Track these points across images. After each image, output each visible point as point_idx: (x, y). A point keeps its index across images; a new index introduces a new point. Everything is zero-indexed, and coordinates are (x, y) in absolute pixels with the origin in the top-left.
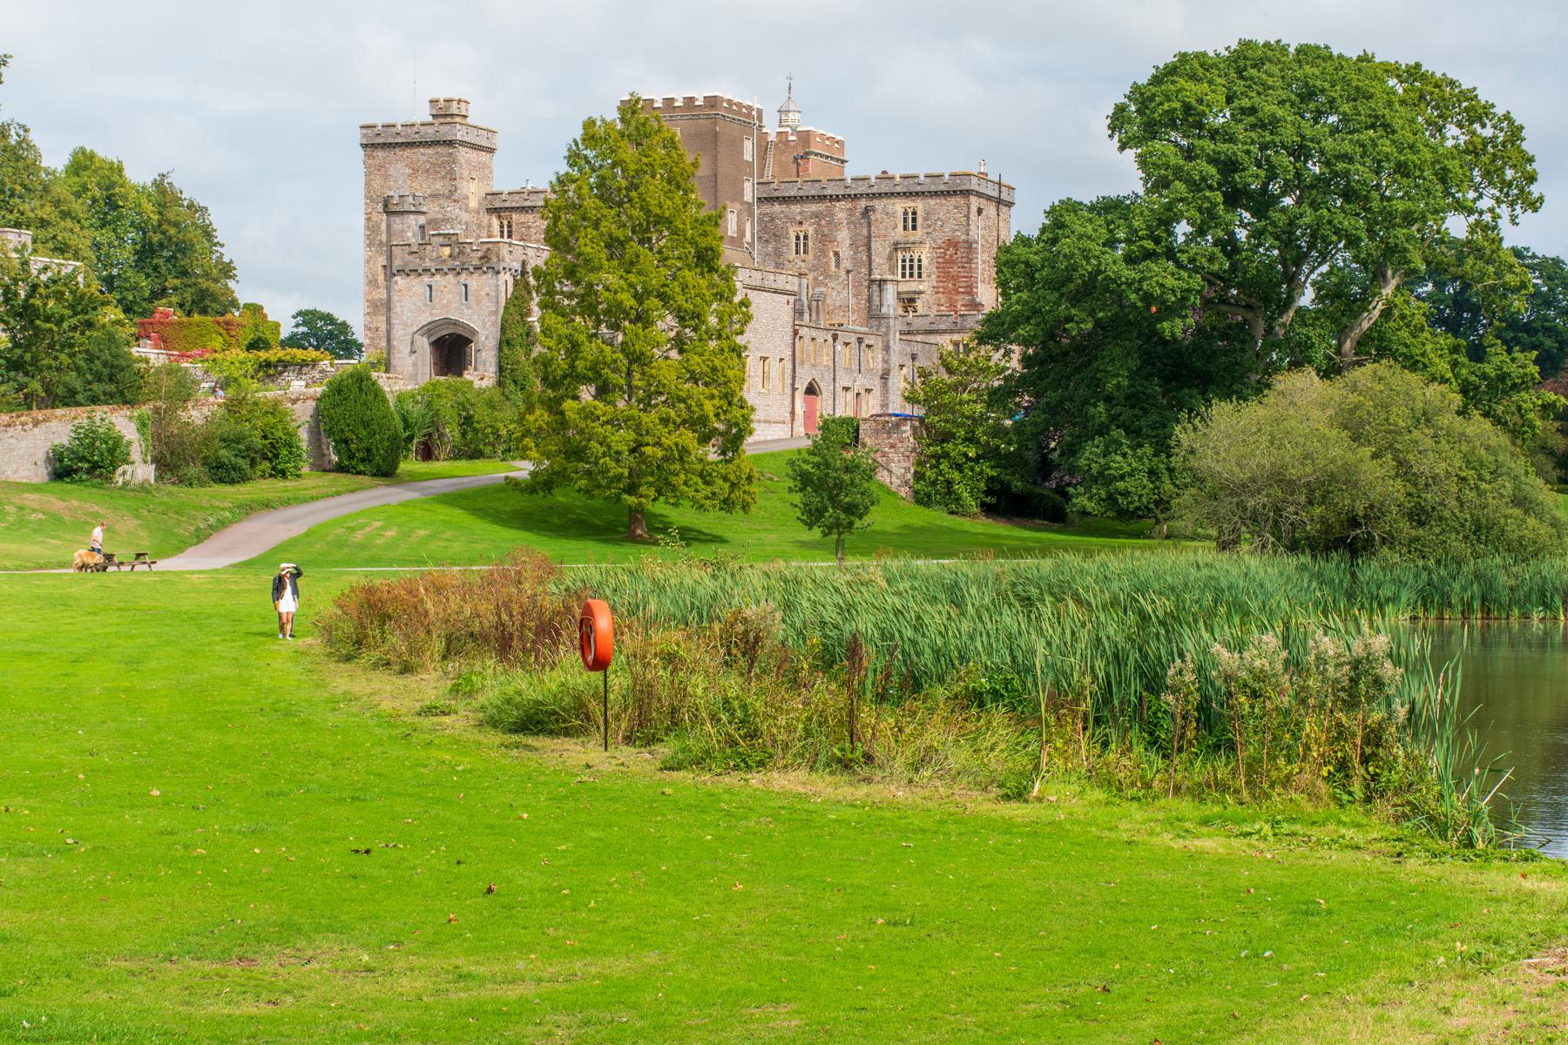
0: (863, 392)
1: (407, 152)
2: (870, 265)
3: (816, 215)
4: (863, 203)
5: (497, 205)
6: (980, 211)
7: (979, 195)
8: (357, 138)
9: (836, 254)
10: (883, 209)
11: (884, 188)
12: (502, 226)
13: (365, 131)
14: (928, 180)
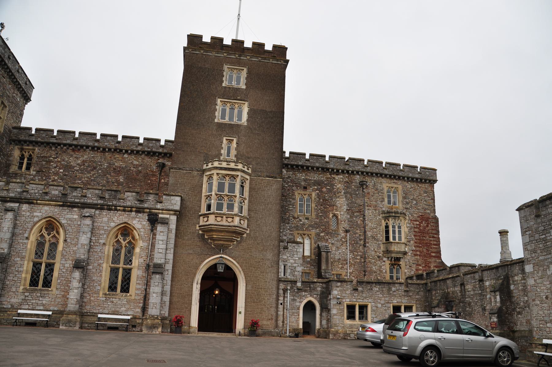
2: (364, 227)
3: (319, 183)
4: (358, 178)
5: (22, 138)
9: (335, 216)
10: (374, 185)
11: (375, 169)
12: (22, 158)
14: (407, 169)
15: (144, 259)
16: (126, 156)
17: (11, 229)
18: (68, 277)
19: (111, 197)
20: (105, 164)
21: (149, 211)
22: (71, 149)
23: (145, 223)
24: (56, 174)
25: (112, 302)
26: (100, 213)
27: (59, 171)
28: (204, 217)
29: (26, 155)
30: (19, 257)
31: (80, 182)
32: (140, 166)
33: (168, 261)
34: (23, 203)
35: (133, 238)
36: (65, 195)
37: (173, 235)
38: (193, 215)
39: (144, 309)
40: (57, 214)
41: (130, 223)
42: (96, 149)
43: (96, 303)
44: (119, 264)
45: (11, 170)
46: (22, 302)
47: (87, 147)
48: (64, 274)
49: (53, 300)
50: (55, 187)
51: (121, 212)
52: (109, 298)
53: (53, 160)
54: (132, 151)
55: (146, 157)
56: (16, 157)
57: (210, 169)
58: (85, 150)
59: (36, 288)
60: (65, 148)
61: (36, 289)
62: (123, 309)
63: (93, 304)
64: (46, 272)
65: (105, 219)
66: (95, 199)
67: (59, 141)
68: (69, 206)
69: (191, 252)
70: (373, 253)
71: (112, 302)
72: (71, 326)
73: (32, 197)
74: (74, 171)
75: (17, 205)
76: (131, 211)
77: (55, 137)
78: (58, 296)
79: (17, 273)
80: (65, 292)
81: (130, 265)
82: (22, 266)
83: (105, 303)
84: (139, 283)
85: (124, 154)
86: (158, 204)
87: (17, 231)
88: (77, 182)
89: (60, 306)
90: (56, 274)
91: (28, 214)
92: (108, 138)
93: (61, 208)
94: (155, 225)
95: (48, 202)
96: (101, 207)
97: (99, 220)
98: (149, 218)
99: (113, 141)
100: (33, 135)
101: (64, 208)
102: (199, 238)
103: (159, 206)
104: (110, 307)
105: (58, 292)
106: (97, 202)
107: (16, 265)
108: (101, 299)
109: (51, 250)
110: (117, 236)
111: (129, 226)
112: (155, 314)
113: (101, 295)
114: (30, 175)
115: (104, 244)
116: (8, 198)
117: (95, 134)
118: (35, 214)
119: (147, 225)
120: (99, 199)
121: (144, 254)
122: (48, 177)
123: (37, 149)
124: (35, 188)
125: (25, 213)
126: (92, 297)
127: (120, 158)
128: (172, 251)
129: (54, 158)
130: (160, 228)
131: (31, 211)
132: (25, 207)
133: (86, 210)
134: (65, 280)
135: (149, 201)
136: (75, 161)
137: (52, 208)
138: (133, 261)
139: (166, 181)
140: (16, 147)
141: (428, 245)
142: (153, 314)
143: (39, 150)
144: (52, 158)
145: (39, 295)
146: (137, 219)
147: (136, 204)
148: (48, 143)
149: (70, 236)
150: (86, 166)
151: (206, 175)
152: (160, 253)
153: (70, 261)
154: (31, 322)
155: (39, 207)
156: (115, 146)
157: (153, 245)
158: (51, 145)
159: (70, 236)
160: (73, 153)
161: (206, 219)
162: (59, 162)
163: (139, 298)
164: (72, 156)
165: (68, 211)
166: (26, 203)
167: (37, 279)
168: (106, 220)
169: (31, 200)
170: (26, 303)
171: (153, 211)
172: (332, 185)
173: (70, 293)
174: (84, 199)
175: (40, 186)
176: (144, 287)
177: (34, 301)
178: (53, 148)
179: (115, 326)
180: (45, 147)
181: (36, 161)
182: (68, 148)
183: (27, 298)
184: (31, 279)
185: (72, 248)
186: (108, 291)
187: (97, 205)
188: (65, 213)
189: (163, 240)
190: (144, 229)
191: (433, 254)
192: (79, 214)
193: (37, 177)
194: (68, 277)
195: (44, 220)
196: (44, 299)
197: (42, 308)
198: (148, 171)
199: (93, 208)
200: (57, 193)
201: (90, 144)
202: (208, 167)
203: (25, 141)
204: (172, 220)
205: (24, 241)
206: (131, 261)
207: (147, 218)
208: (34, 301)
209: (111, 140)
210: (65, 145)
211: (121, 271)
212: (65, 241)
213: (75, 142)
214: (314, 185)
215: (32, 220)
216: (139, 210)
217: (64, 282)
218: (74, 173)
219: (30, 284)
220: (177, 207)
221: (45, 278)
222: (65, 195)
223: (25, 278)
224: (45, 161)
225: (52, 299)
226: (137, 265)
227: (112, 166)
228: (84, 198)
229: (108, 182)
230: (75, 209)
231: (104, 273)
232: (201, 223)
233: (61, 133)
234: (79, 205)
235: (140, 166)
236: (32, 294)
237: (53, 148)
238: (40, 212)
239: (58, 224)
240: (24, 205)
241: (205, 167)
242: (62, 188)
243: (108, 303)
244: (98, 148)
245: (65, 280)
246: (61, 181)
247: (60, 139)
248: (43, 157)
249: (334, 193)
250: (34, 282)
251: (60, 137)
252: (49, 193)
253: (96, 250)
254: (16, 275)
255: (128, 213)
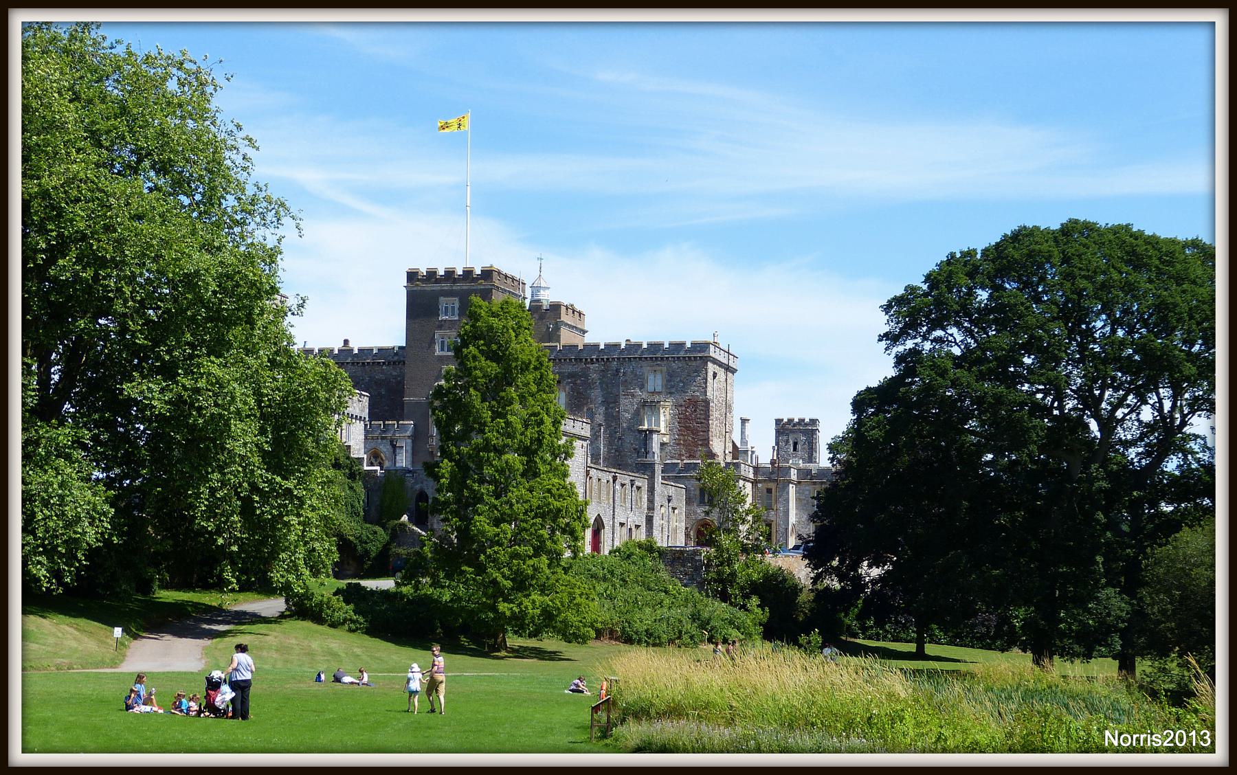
0: (633, 528)
6: (715, 375)
7: (715, 361)
16: (384, 367)
35: (382, 459)
70: (629, 445)
141: (695, 432)
172: (586, 376)
191: (700, 443)
214: (569, 378)
249: (588, 385)
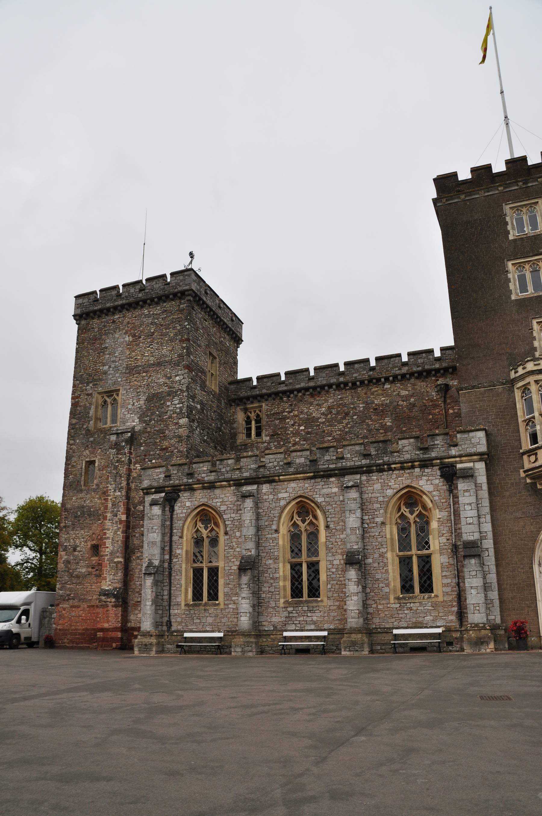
1: (129, 316)
5: (243, 394)
8: (70, 308)
12: (248, 421)
13: (80, 301)
15: (448, 538)
16: (387, 386)
17: (254, 521)
18: (340, 579)
19: (379, 452)
20: (361, 406)
21: (441, 462)
22: (308, 395)
23: (437, 481)
24: (297, 433)
25: (411, 609)
26: (369, 478)
27: (299, 428)
28: (529, 456)
29: (253, 416)
30: (271, 559)
31: (330, 438)
32: (412, 396)
33: (485, 534)
34: (262, 484)
35: (424, 507)
36: (314, 462)
37: (484, 493)
38: (510, 455)
39: (461, 615)
40: (309, 490)
41: (416, 486)
42: (342, 386)
43: (387, 613)
44: (410, 550)
45: (239, 441)
46: (286, 621)
47: (330, 386)
48: (334, 576)
49: (326, 615)
50: (298, 453)
51: (397, 472)
52: (404, 603)
53: (288, 415)
54: (395, 377)
55: (417, 381)
56: (241, 422)
57: (522, 377)
58: (327, 392)
59: (301, 599)
60: (300, 394)
61: (301, 601)
62: (429, 618)
63: (382, 615)
64: (309, 576)
65: (377, 486)
66: (357, 459)
67: (290, 387)
68: (322, 477)
69: (519, 514)
71: (411, 609)
72: (357, 651)
73: (272, 472)
74: (319, 425)
75: (255, 487)
76: (413, 467)
77: (283, 382)
78: (332, 608)
79: (272, 581)
80: (340, 601)
81: (427, 549)
82: (277, 570)
83: (400, 612)
84: (445, 576)
85: (384, 384)
86: (452, 448)
87: (262, 523)
88: (326, 439)
89: (337, 622)
90: (323, 577)
91: (271, 497)
92: (356, 366)
93: (313, 481)
94: (454, 482)
95: (293, 476)
96: (368, 469)
97: (369, 488)
98: (441, 472)
99: (364, 369)
100: (255, 387)
101: (317, 480)
102: (528, 491)
103: (454, 451)
104: (408, 617)
105: (330, 603)
106: (360, 463)
107: (269, 571)
108: (393, 606)
109: (311, 543)
110: (399, 509)
111: (415, 491)
112: (480, 621)
113: (392, 601)
114: (263, 443)
115: (383, 523)
116: (242, 480)
117: (337, 365)
118: (280, 496)
119: (441, 484)
120: (362, 457)
121: (445, 530)
122: (287, 441)
123: (264, 404)
124: (273, 460)
125: (267, 497)
126: (380, 604)
127: (380, 392)
128: (488, 517)
129: (289, 412)
130: (462, 485)
131: (275, 492)
132: (265, 488)
133: (347, 478)
134: (337, 584)
135: (436, 446)
136: (317, 410)
137: (301, 484)
138: (431, 542)
139: (456, 411)
140: (238, 408)
142: (476, 622)
143: (267, 405)
144: (286, 414)
145: (306, 609)
146: (425, 478)
147: (418, 455)
148: (277, 394)
149: (333, 519)
150: (334, 414)
151: (518, 388)
152: (470, 524)
153: (339, 556)
154: (302, 648)
155: (283, 486)
156: (369, 376)
157: (457, 514)
158: (281, 395)
159: (333, 519)
160: (312, 400)
161: (533, 458)
162: (296, 416)
163: (450, 598)
164: (311, 404)
165: (323, 483)
166: (265, 482)
167: (300, 586)
168: (379, 488)
169: (271, 476)
170: (292, 622)
171: (447, 460)
173: (348, 603)
174: (342, 463)
175: (279, 456)
176: (455, 581)
177: (302, 619)
178: (284, 399)
179: (421, 645)
180: (274, 399)
181: (267, 422)
182: (304, 395)
183: (291, 615)
184: (292, 588)
185: (338, 537)
186: (402, 593)
187: (361, 467)
188: (320, 487)
189: (470, 504)
190: (437, 491)
192: (339, 485)
193: (272, 444)
194: (340, 579)
195: (294, 503)
196: (314, 614)
197: (313, 627)
198: (424, 401)
199: (357, 473)
200: (302, 460)
201: (333, 380)
202: (517, 375)
203: (248, 398)
204: (478, 469)
205: (273, 536)
206: (427, 543)
207: (439, 473)
208: (302, 619)
209: (360, 367)
210: (299, 390)
211: (415, 560)
212: (327, 527)
213: (312, 384)
215: (278, 505)
216: (425, 464)
217: (337, 587)
218: (320, 427)
219: (292, 595)
220: (483, 448)
221: (310, 584)
222: (314, 462)
223: (284, 587)
224: (278, 419)
225: (325, 613)
226: (437, 547)
227: (370, 406)
228: (341, 461)
229: (370, 431)
230: (332, 479)
231: (390, 568)
232: (527, 466)
233: (291, 376)
234: (337, 472)
235: (412, 396)
236: (296, 609)
237: (284, 399)
238: (286, 492)
239: (313, 505)
240: (264, 485)
241: (513, 375)
242: (308, 453)
243: (406, 612)
244: (346, 384)
245: (337, 584)
246: (304, 442)
247: (290, 383)
248: (274, 414)
250: (296, 592)
251: (291, 381)
252: (293, 463)
253: (373, 534)
254: (272, 584)
255: (408, 471)
